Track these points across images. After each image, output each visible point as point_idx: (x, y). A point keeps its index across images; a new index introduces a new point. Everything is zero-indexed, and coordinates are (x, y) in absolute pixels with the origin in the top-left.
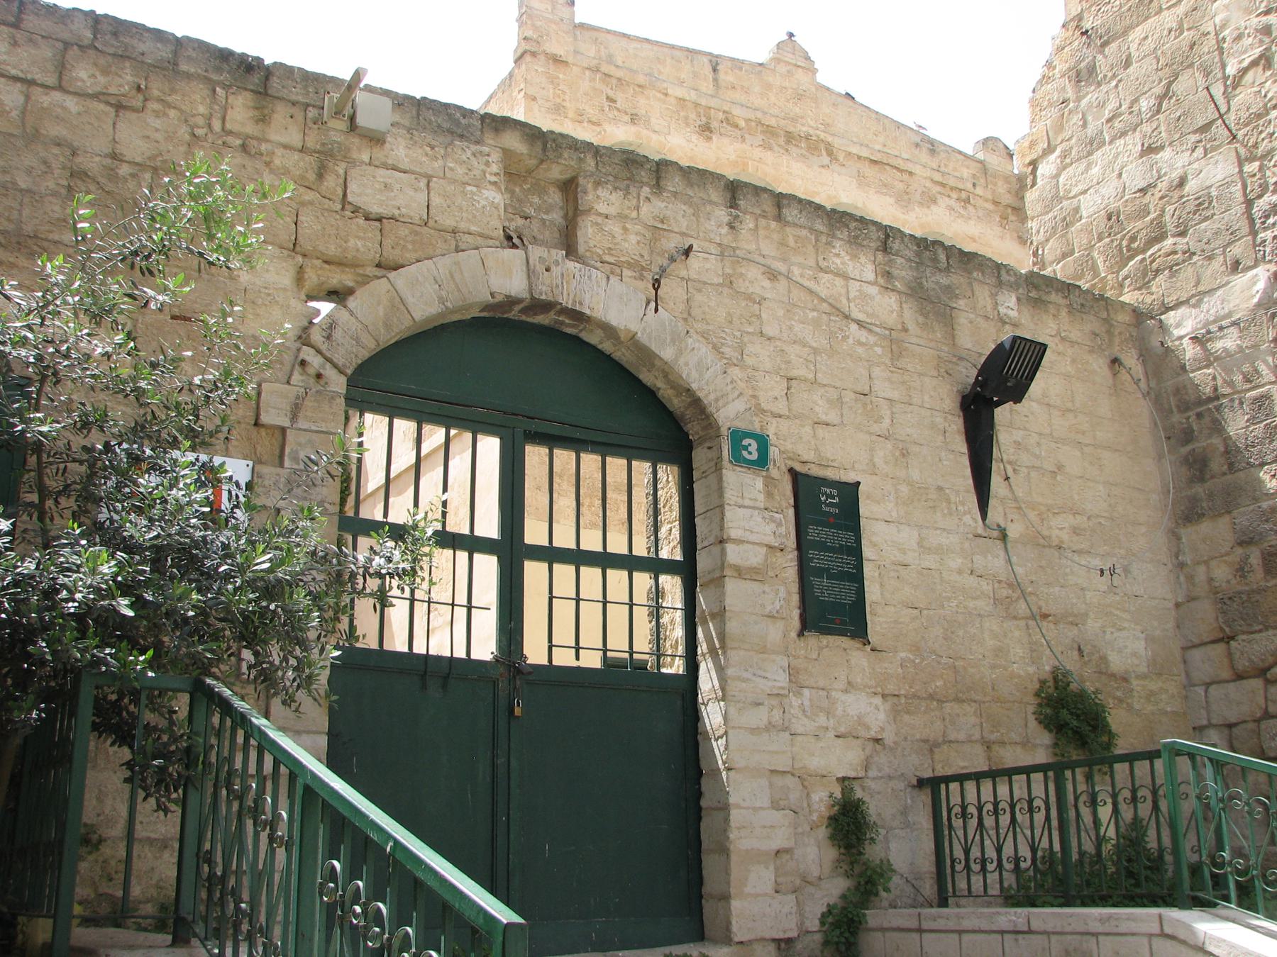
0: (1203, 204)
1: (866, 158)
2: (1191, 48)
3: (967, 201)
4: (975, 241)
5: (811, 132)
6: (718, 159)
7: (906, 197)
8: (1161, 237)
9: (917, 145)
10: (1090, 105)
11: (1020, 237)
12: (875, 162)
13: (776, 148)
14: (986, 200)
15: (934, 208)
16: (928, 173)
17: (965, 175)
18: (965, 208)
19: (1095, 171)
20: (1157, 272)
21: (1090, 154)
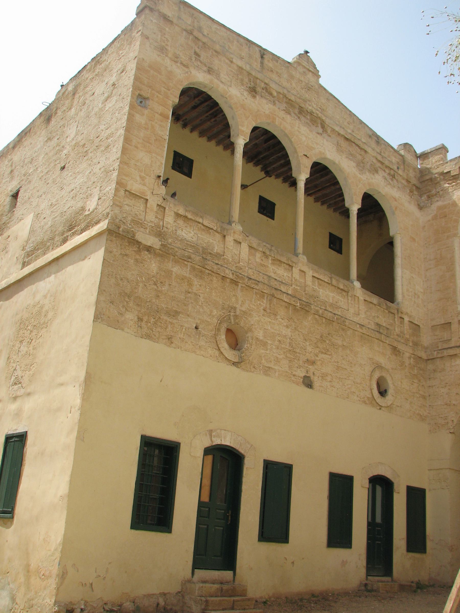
1: (342, 136)
3: (393, 176)
4: (396, 201)
5: (314, 111)
6: (258, 110)
7: (362, 165)
9: (370, 137)
11: (418, 205)
12: (347, 139)
13: (293, 114)
14: (403, 179)
15: (376, 175)
16: (375, 154)
17: (394, 161)
18: (392, 180)
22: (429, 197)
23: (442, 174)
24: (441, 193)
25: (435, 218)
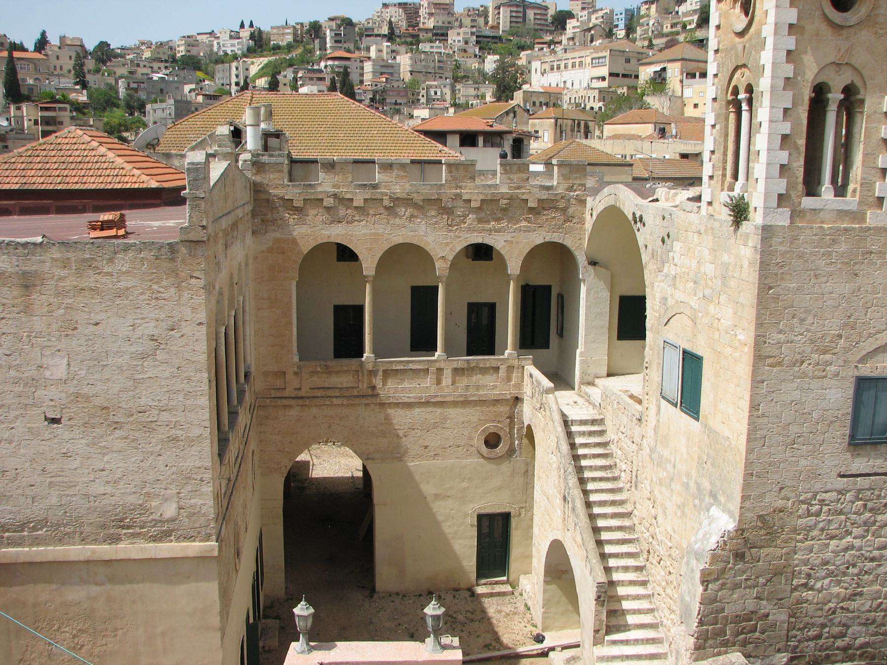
0: (773, 625)
8: (755, 631)
10: (739, 569)
19: (735, 596)
20: (750, 643)
22: (263, 221)
23: (282, 198)
24: (280, 222)
25: (270, 250)
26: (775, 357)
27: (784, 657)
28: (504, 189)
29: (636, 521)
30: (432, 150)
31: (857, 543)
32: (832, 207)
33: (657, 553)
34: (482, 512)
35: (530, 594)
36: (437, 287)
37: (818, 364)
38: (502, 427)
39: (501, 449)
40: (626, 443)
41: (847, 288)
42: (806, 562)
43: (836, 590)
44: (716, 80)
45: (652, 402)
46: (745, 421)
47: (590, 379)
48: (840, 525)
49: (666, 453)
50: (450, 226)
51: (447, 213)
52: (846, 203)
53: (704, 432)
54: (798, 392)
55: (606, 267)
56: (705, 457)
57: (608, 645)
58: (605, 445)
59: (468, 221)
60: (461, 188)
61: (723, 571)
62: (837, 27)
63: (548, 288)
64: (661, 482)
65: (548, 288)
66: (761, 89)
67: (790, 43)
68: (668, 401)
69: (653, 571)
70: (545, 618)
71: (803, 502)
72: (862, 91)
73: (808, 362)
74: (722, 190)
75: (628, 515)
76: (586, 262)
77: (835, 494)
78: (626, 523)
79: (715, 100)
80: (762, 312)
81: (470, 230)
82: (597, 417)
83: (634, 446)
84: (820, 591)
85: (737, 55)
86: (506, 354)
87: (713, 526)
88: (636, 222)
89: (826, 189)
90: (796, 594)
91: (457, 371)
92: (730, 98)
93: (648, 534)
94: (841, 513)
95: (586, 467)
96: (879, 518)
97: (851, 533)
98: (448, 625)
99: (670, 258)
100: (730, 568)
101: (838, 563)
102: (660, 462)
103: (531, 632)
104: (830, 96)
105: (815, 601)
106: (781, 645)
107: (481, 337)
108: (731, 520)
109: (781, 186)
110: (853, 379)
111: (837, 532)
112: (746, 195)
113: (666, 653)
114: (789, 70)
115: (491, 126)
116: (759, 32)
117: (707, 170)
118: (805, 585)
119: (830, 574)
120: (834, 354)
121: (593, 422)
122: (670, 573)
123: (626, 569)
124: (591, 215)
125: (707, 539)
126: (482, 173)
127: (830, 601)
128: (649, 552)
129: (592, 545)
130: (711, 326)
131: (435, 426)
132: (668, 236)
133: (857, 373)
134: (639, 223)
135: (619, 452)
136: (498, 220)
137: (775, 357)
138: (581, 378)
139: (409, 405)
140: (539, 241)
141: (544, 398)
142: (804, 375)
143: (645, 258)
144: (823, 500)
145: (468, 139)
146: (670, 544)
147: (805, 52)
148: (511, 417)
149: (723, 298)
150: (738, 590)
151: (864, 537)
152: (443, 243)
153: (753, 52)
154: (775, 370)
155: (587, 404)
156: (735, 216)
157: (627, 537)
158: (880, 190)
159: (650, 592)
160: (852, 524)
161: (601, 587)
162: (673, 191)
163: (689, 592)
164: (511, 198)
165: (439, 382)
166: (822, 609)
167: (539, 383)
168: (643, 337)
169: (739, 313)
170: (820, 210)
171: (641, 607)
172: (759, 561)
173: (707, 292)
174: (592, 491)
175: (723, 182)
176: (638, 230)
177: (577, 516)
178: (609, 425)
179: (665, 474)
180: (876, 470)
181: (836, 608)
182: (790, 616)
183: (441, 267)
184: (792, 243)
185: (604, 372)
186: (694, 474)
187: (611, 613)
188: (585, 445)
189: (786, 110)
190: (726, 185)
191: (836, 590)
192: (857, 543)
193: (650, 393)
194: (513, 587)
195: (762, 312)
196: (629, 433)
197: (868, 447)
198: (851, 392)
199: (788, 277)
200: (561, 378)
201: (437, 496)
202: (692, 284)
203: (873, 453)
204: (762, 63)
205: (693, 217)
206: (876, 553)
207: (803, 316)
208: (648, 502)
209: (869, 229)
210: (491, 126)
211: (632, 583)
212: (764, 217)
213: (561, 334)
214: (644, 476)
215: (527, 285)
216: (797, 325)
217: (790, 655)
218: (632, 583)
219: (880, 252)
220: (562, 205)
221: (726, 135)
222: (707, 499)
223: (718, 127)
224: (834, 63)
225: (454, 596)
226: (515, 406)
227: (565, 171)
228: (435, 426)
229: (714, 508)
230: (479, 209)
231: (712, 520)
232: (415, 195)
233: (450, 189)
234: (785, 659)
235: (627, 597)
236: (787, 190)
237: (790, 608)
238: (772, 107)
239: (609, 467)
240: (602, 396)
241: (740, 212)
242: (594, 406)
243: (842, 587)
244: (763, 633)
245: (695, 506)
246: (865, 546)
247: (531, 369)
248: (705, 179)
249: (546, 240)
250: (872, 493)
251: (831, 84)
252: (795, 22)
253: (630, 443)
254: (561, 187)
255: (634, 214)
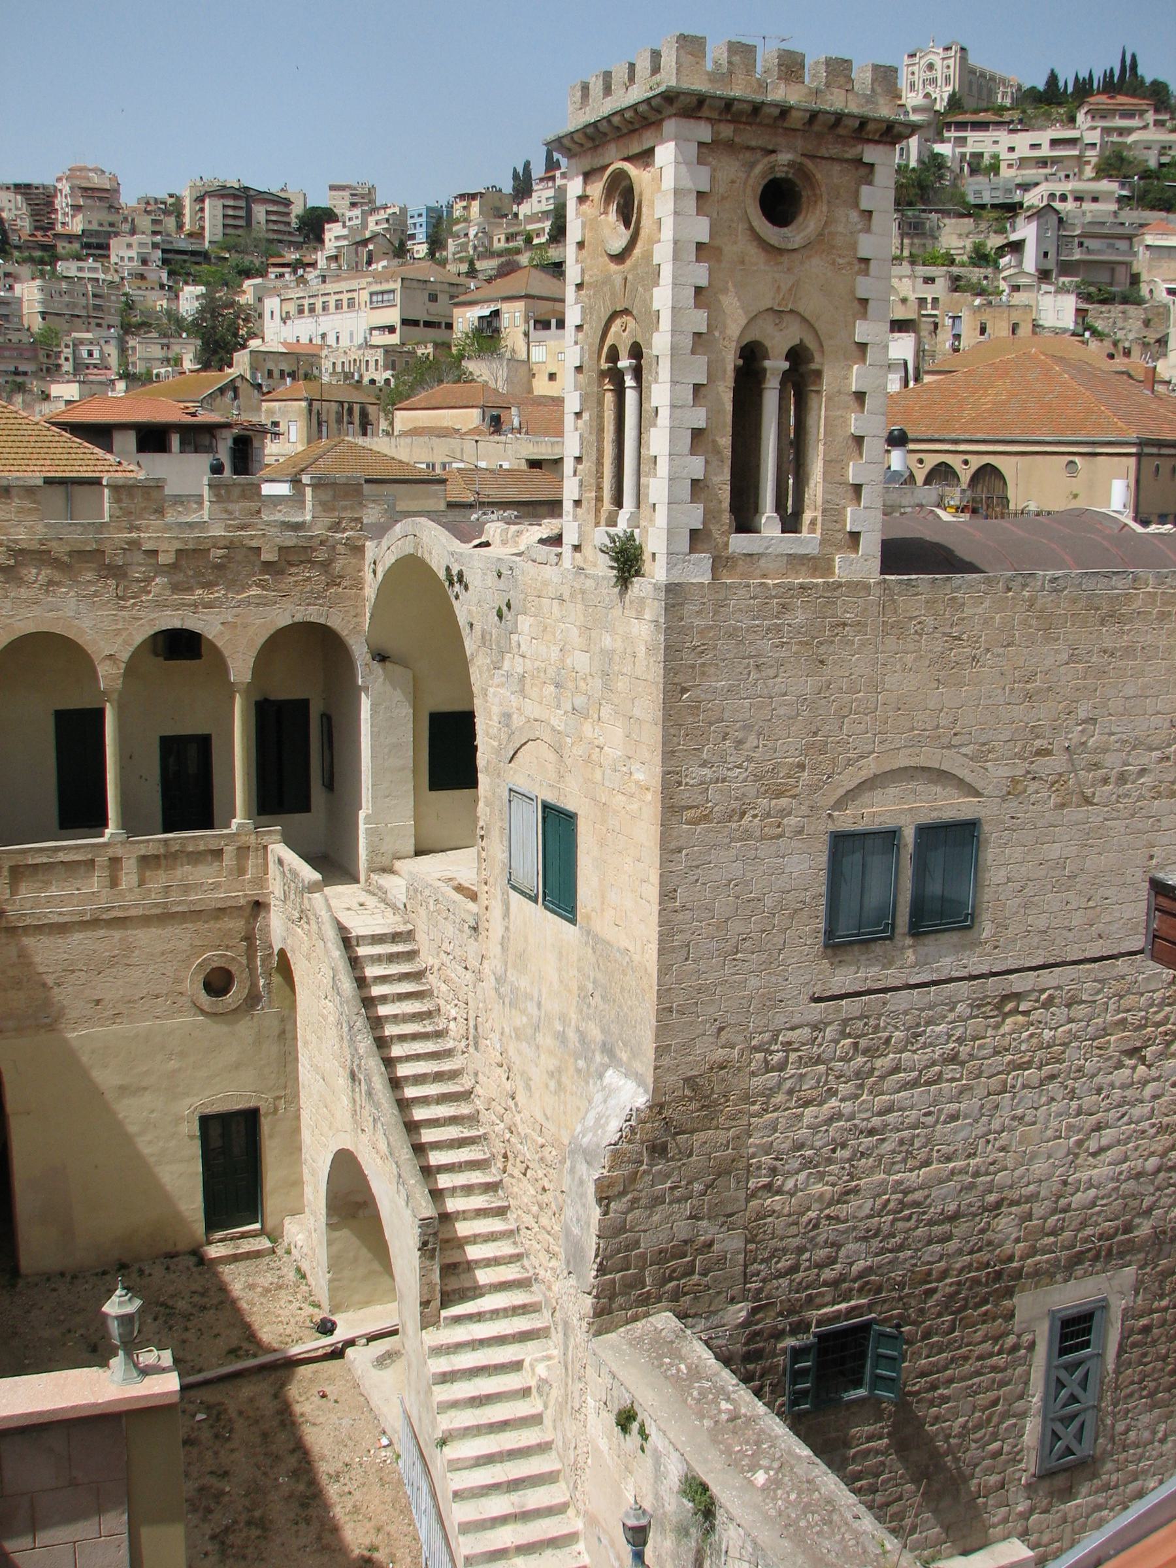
2: (733, 1161)
8: (692, 1273)
10: (660, 1172)
19: (656, 1218)
20: (685, 1294)
21: (654, 1206)
26: (697, 807)
27: (741, 1310)
28: (218, 531)
29: (480, 1104)
30: (87, 460)
31: (847, 1107)
32: (779, 550)
33: (520, 1158)
34: (208, 1111)
35: (305, 1250)
36: (101, 713)
37: (768, 815)
38: (232, 956)
39: (235, 995)
40: (455, 972)
41: (809, 686)
42: (767, 1149)
43: (817, 1188)
44: (581, 335)
45: (494, 896)
46: (655, 919)
47: (385, 861)
48: (818, 1082)
49: (524, 983)
50: (121, 598)
51: (114, 576)
52: (801, 542)
53: (587, 943)
54: (739, 864)
55: (403, 663)
56: (590, 986)
57: (446, 1326)
58: (417, 976)
59: (154, 590)
60: (138, 529)
61: (633, 1178)
62: (773, 251)
63: (303, 706)
64: (518, 1034)
65: (303, 706)
66: (655, 352)
67: (700, 274)
68: (522, 893)
69: (515, 1189)
70: (334, 1287)
71: (756, 1049)
72: (817, 357)
73: (752, 812)
74: (597, 524)
75: (466, 1096)
76: (369, 656)
77: (807, 1030)
78: (464, 1109)
79: (579, 369)
80: (672, 731)
81: (159, 605)
82: (402, 928)
83: (469, 975)
84: (792, 1195)
85: (613, 294)
86: (234, 826)
87: (612, 1102)
88: (451, 584)
89: (768, 519)
90: (754, 1203)
91: (147, 862)
92: (605, 366)
93: (502, 1125)
94: (818, 1061)
95: (387, 1017)
96: (878, 1063)
97: (835, 1094)
98: (160, 1321)
99: (514, 644)
100: (644, 1172)
101: (818, 1144)
102: (514, 1000)
103: (311, 1316)
104: (767, 364)
105: (786, 1211)
106: (736, 1290)
107: (187, 799)
108: (641, 1090)
109: (695, 516)
110: (826, 837)
111: (815, 1093)
112: (637, 531)
113: (547, 1329)
114: (699, 320)
115: (194, 415)
116: (648, 256)
117: (570, 490)
118: (768, 1187)
119: (807, 1164)
120: (794, 797)
121: (395, 937)
122: (544, 1190)
123: (468, 1190)
124: (374, 572)
125: (603, 1127)
126: (178, 500)
127: (809, 1209)
128: (505, 1156)
129: (406, 1153)
130: (588, 760)
131: (112, 962)
132: (509, 606)
133: (832, 828)
134: (457, 585)
135: (444, 987)
136: (208, 585)
137: (697, 807)
138: (370, 861)
139: (62, 928)
140: (284, 621)
141: (306, 901)
142: (747, 835)
143: (470, 645)
144: (789, 1043)
145: (152, 438)
146: (541, 1141)
147: (725, 291)
148: (249, 938)
149: (606, 711)
150: (661, 1207)
151: (857, 1097)
152: (109, 630)
153: (640, 289)
154: (699, 828)
155: (382, 905)
156: (619, 569)
157: (467, 1133)
158: (853, 521)
159: (513, 1226)
160: (837, 1078)
161: (428, 1225)
162: (513, 528)
163: (578, 1220)
164: (231, 546)
165: (114, 883)
166: (796, 1224)
167: (295, 874)
168: (473, 783)
169: (634, 736)
170: (760, 555)
171: (499, 1254)
172: (690, 1155)
173: (580, 701)
174: (400, 1059)
175: (598, 511)
176: (457, 597)
177: (377, 1106)
178: (423, 942)
179: (525, 1020)
180: (870, 985)
181: (818, 1218)
182: (747, 1241)
183: (108, 675)
184: (716, 613)
185: (411, 849)
186: (573, 1016)
187: (449, 1270)
188: (384, 979)
189: (697, 388)
190: (604, 516)
191: (817, 1188)
192: (847, 1107)
193: (491, 881)
194: (273, 1240)
195: (672, 731)
196: (458, 952)
197: (856, 948)
198: (823, 859)
199: (713, 670)
200: (333, 862)
201: (123, 1090)
202: (552, 688)
203: (864, 957)
204: (655, 307)
205: (549, 572)
206: (876, 1121)
207: (739, 735)
208: (499, 1070)
209: (840, 585)
210: (194, 415)
211: (481, 1213)
212: (668, 570)
213: (330, 784)
214: (488, 1025)
215: (266, 700)
216: (732, 750)
217: (750, 1305)
218: (481, 1213)
219: (859, 623)
220: (321, 555)
221: (601, 430)
222: (598, 1058)
223: (586, 416)
224: (772, 309)
225: (168, 1268)
226: (255, 916)
227: (326, 496)
228: (112, 962)
229: (610, 1072)
230: (174, 567)
231: (609, 1093)
232: (54, 544)
233: (120, 530)
234: (744, 1313)
235: (474, 1239)
236: (704, 523)
237: (746, 1228)
238: (674, 382)
239: (429, 1015)
240: (411, 888)
241: (627, 561)
242: (395, 908)
243: (827, 1184)
244: (705, 1275)
245: (579, 1071)
246: (859, 1112)
247: (280, 850)
248: (568, 506)
249: (296, 620)
250: (866, 1024)
251: (768, 343)
252: (706, 240)
253: (460, 970)
254: (319, 525)
255: (448, 569)
